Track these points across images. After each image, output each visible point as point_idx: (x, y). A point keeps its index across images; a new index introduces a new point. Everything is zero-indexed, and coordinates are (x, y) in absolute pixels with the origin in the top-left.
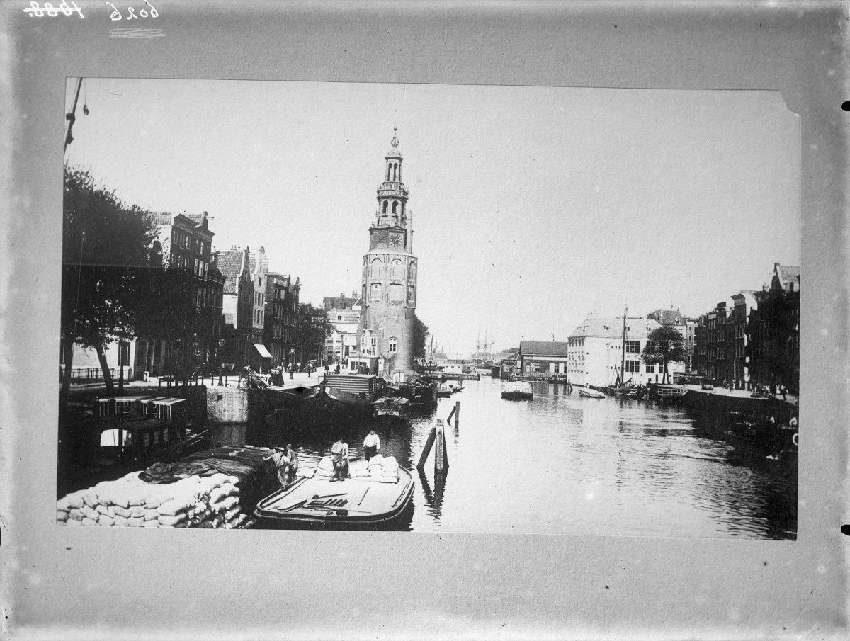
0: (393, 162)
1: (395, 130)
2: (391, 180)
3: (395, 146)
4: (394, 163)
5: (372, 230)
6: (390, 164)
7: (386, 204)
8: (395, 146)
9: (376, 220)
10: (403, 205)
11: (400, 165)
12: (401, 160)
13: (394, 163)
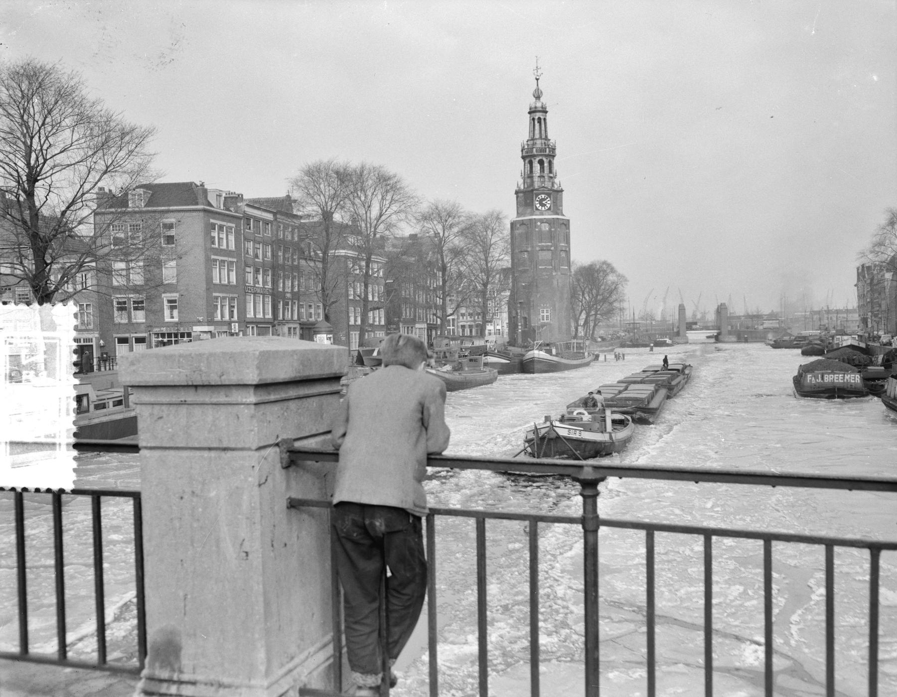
0: (538, 115)
1: (537, 80)
2: (537, 136)
3: (538, 97)
4: (538, 116)
5: (517, 193)
6: (534, 119)
7: (531, 163)
8: (538, 97)
9: (521, 181)
10: (550, 163)
11: (545, 119)
12: (546, 112)
13: (538, 116)
